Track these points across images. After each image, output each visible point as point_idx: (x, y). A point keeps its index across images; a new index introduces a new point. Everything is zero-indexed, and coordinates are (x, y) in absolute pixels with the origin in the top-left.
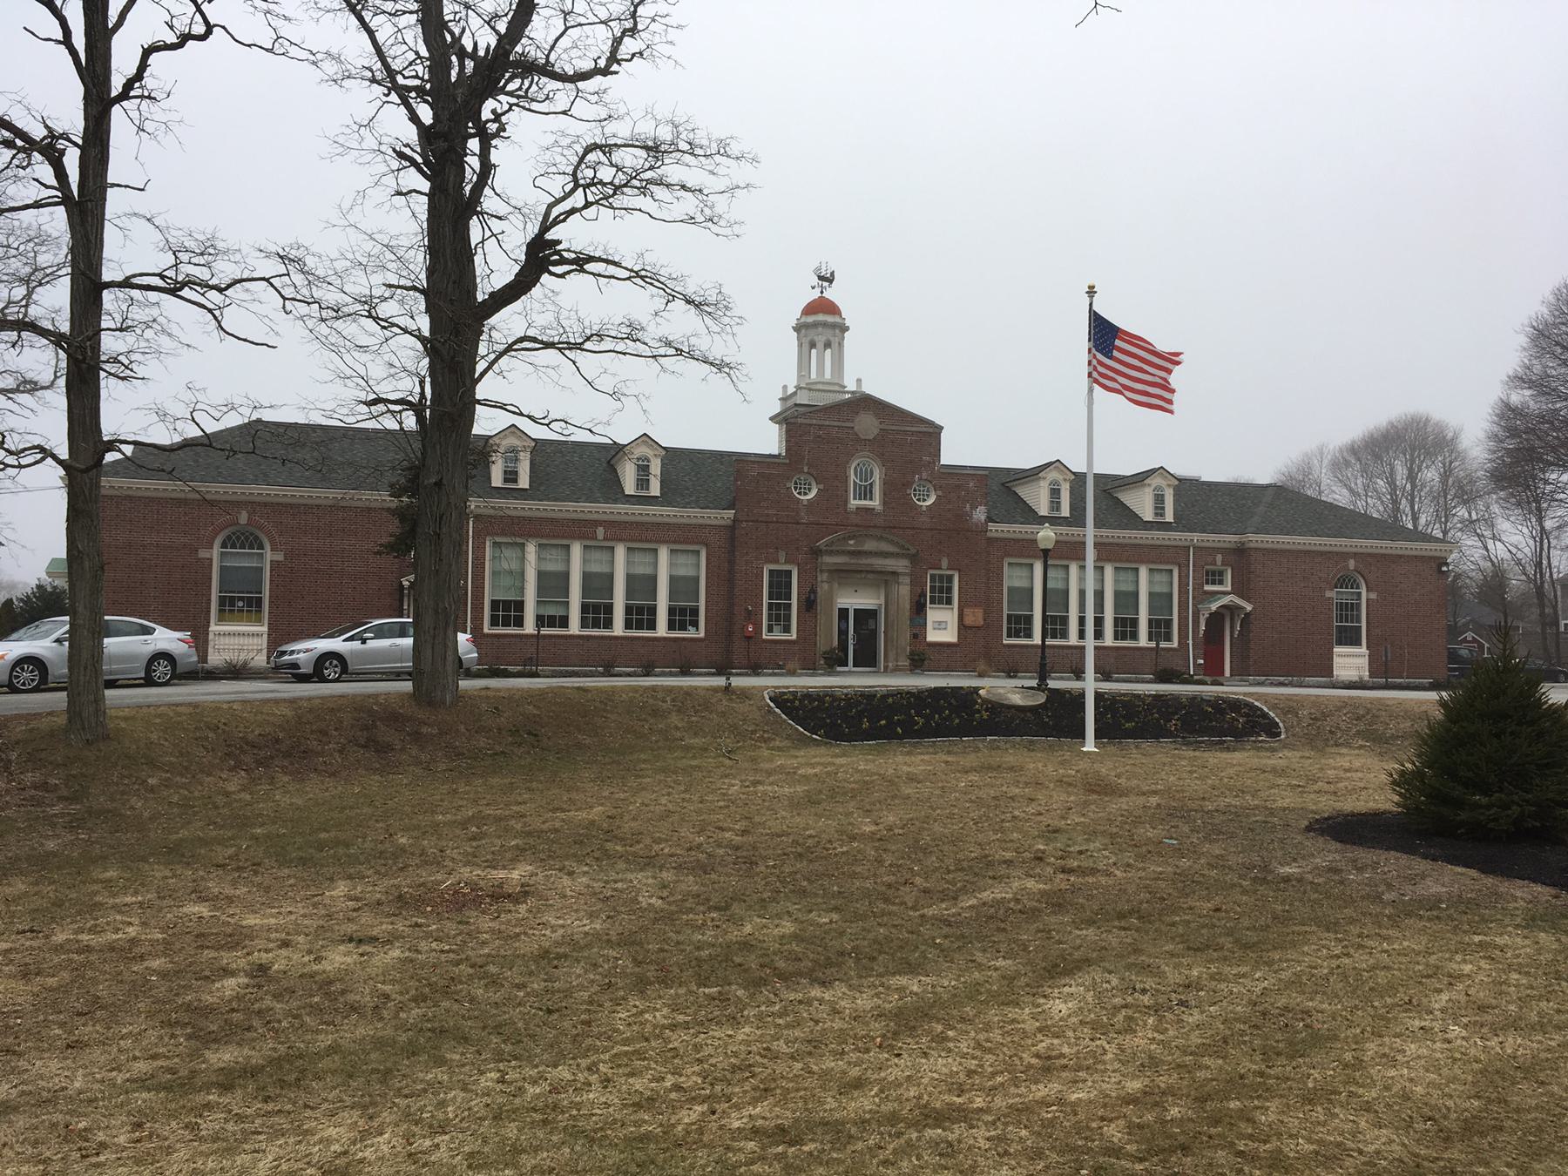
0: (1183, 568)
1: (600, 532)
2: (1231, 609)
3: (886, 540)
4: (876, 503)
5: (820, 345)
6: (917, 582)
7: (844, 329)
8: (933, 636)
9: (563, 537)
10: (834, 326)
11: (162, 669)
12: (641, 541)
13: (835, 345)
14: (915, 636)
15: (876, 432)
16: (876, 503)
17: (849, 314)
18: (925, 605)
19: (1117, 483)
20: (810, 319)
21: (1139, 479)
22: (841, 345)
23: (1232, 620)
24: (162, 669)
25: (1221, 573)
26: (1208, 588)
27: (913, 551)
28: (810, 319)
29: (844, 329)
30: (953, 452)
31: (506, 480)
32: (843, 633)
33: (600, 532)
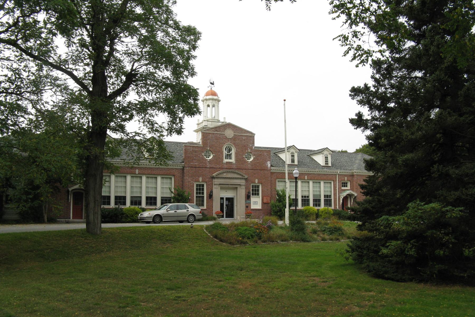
0: (335, 181)
1: (306, 177)
2: (350, 196)
3: (237, 173)
4: (233, 160)
5: (211, 106)
6: (247, 188)
7: (219, 101)
8: (253, 207)
9: (124, 173)
10: (216, 100)
11: (191, 219)
12: (151, 174)
13: (216, 107)
14: (247, 207)
15: (233, 135)
16: (233, 160)
17: (221, 96)
18: (250, 196)
19: (312, 153)
20: (208, 97)
21: (320, 152)
22: (218, 106)
23: (350, 199)
24: (191, 219)
25: (346, 183)
26: (343, 188)
27: (246, 177)
28: (208, 97)
29: (219, 101)
30: (259, 142)
31: (326, 164)
32: (222, 205)
33: (306, 177)
